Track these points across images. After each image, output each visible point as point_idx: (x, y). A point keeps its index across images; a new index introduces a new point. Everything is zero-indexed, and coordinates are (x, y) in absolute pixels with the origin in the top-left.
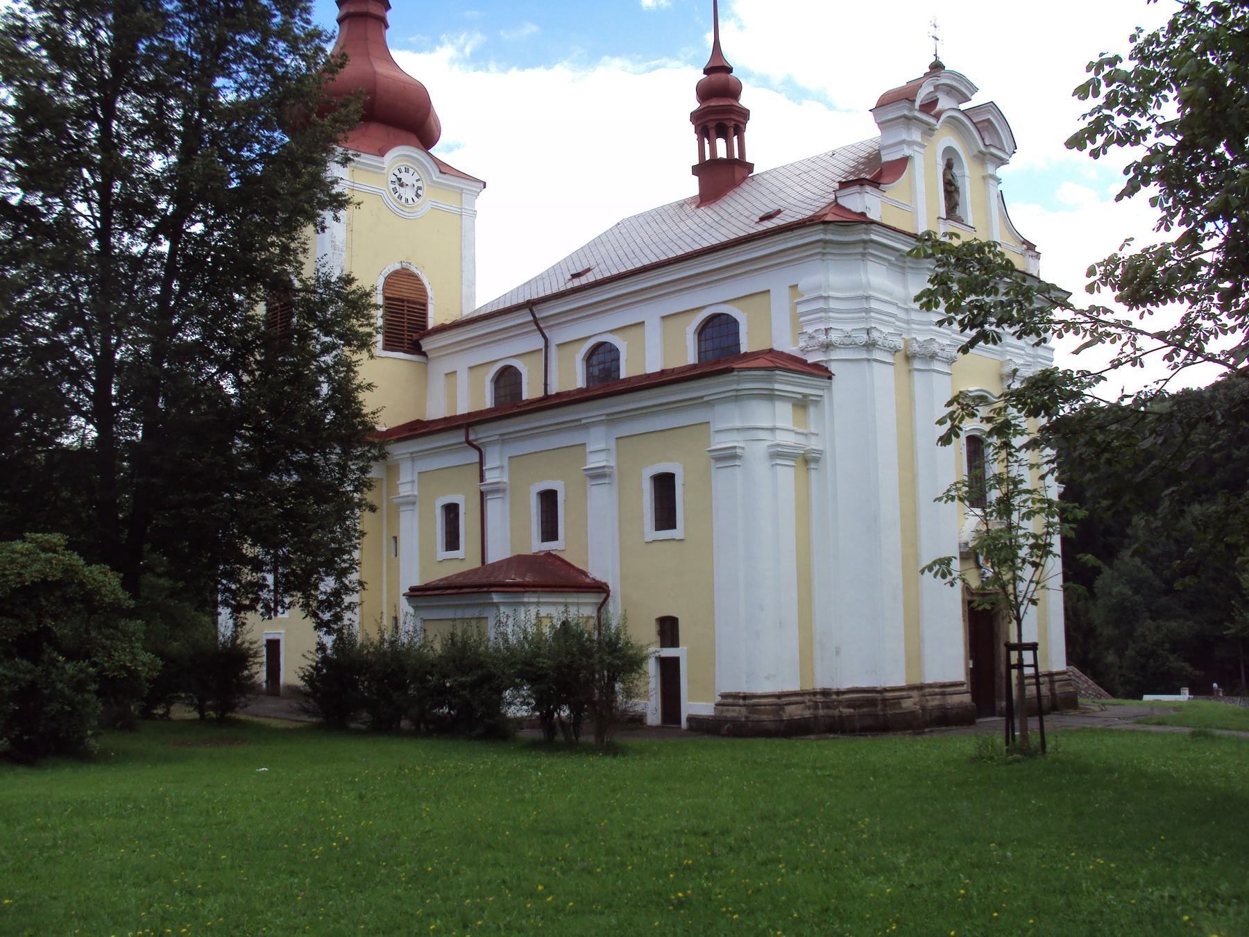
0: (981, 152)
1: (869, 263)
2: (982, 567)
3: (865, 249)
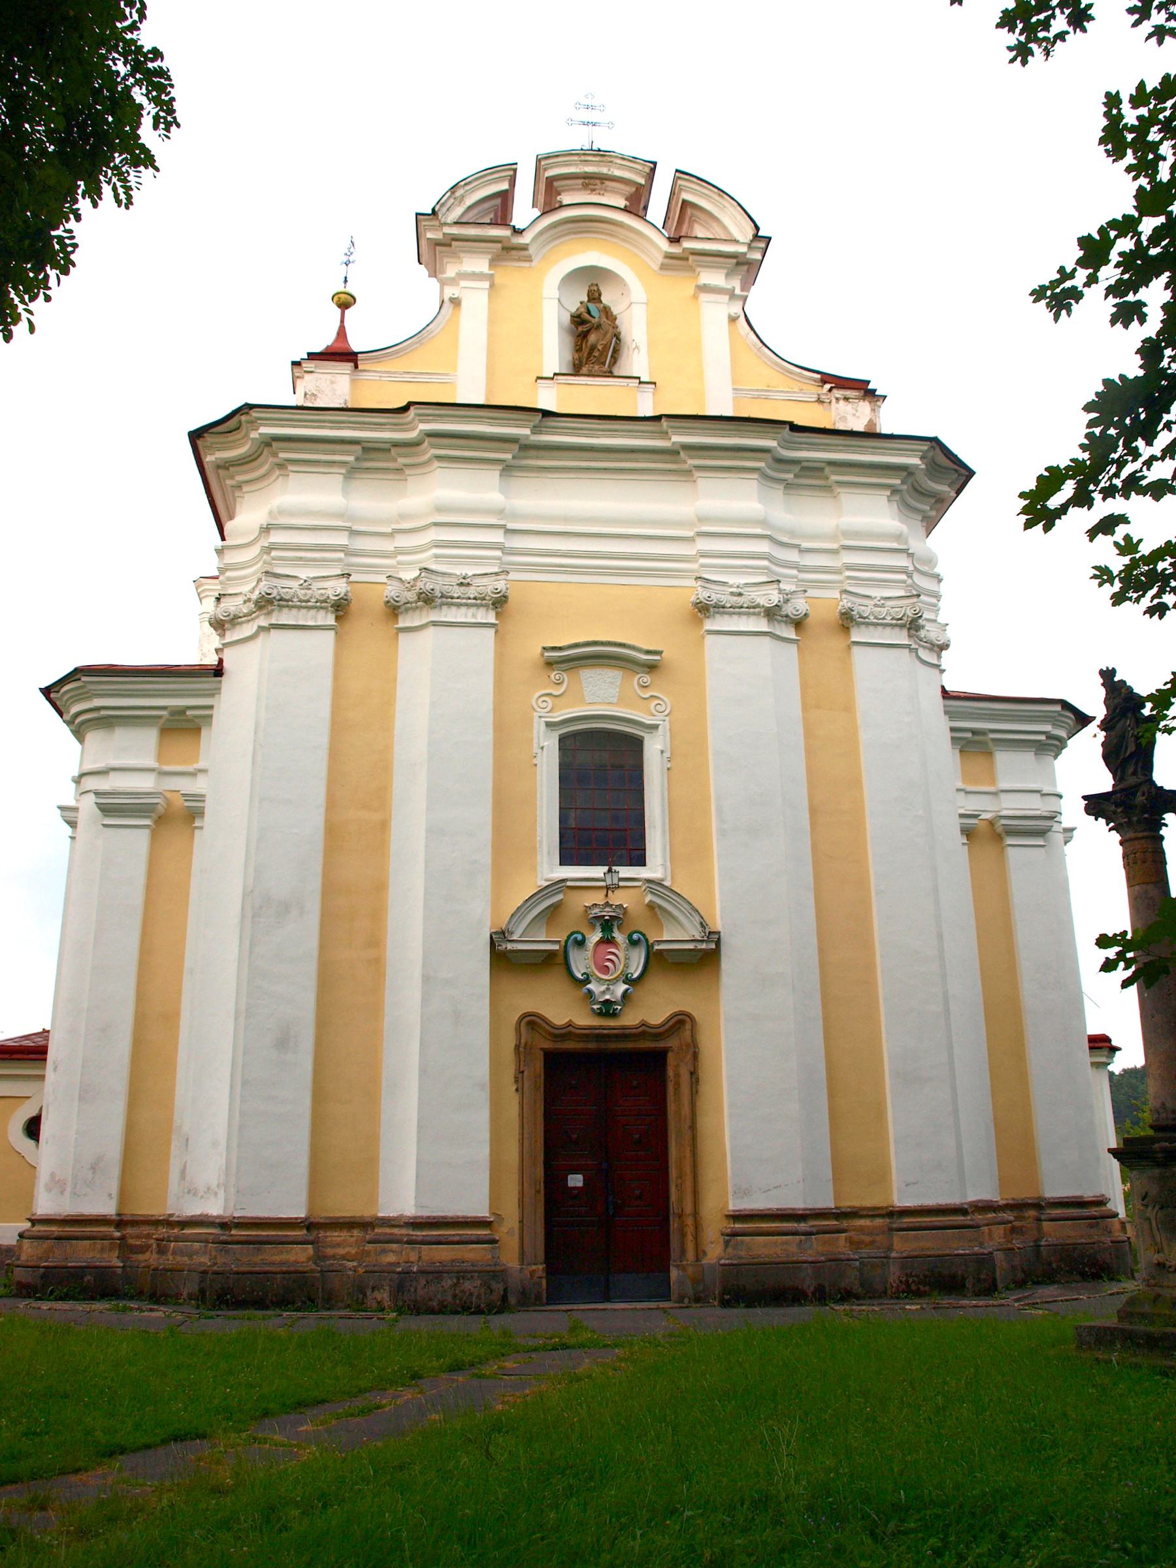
0: (669, 256)
1: (292, 475)
2: (587, 981)
3: (275, 455)
